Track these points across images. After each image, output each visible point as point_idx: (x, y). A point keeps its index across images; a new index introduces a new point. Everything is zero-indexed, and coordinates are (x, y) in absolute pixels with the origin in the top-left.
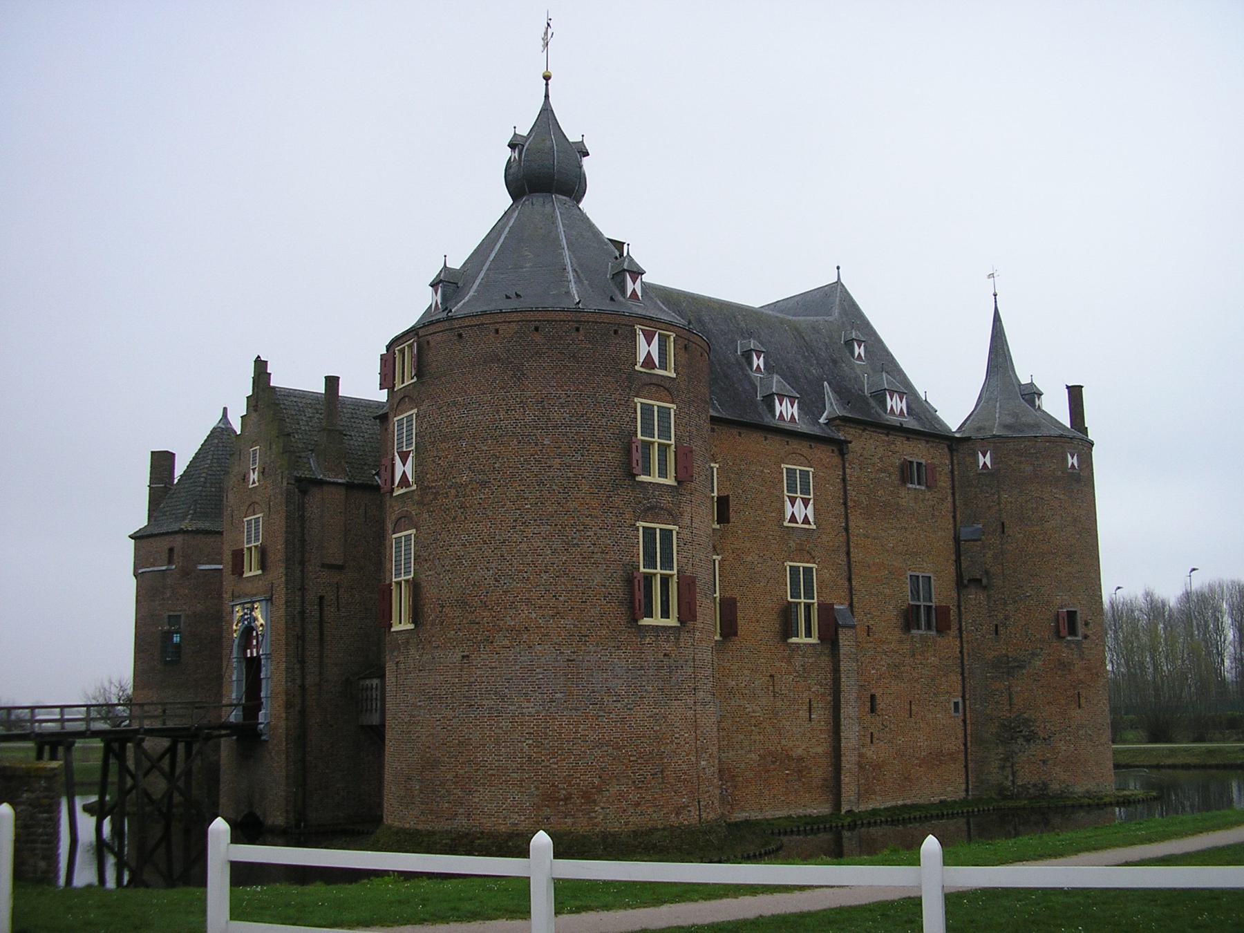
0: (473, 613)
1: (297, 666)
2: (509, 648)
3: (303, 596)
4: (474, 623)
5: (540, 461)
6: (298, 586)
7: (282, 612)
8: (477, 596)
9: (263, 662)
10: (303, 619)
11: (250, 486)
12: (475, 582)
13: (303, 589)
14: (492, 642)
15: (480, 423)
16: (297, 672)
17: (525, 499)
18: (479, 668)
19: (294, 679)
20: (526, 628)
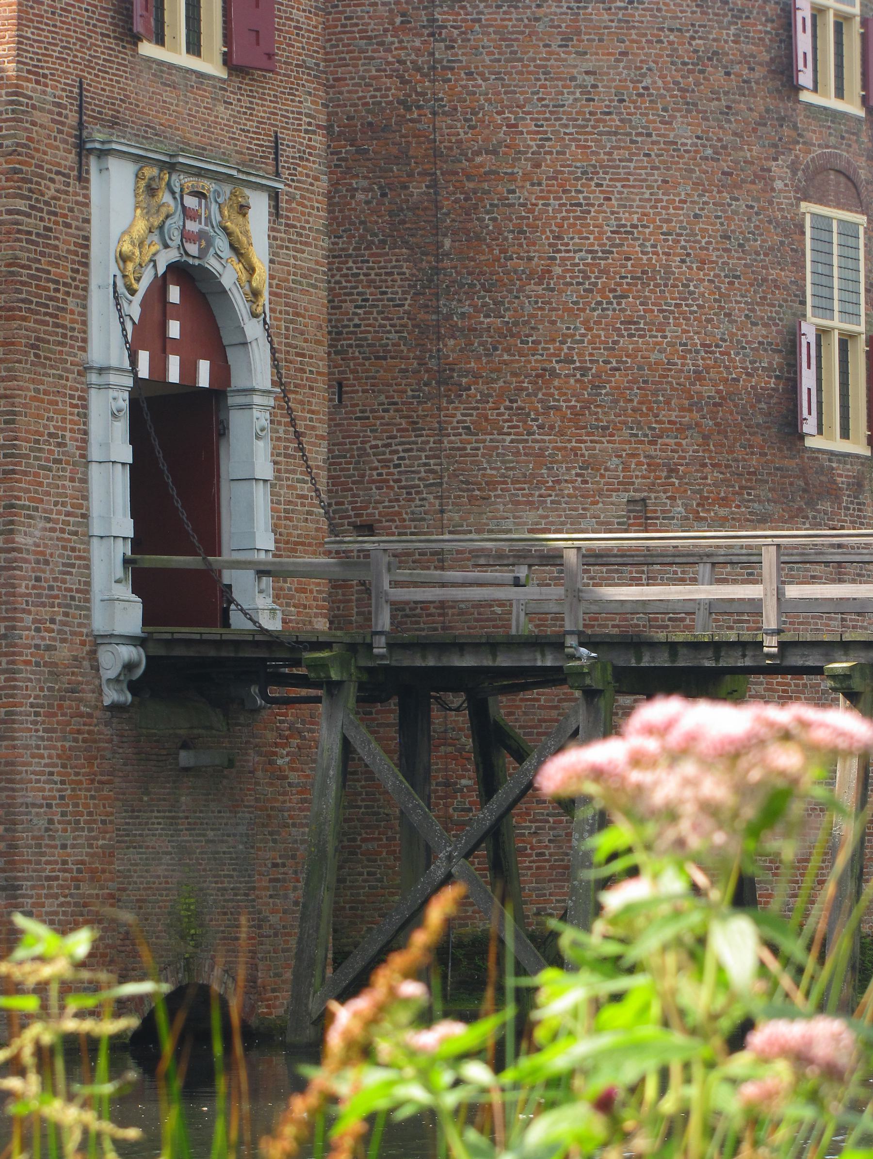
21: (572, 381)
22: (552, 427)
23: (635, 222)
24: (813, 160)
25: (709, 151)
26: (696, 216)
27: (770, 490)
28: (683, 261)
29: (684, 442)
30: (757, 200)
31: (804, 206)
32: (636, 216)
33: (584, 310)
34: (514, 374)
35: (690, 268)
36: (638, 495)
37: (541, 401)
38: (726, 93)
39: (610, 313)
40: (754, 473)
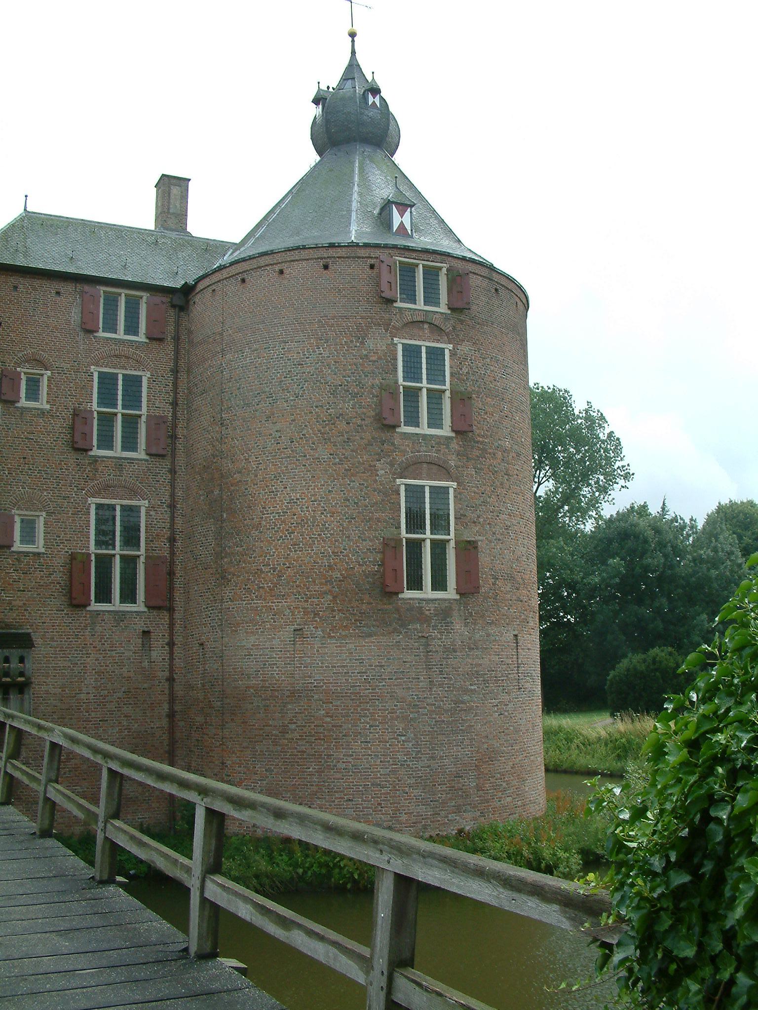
21: (269, 574)
22: (261, 597)
23: (298, 497)
24: (407, 459)
25: (337, 460)
26: (329, 491)
27: (374, 620)
28: (322, 513)
29: (322, 600)
30: (367, 481)
31: (398, 481)
32: (298, 494)
33: (274, 541)
34: (247, 573)
35: (326, 516)
36: (298, 627)
37: (257, 585)
39: (286, 541)
40: (364, 613)
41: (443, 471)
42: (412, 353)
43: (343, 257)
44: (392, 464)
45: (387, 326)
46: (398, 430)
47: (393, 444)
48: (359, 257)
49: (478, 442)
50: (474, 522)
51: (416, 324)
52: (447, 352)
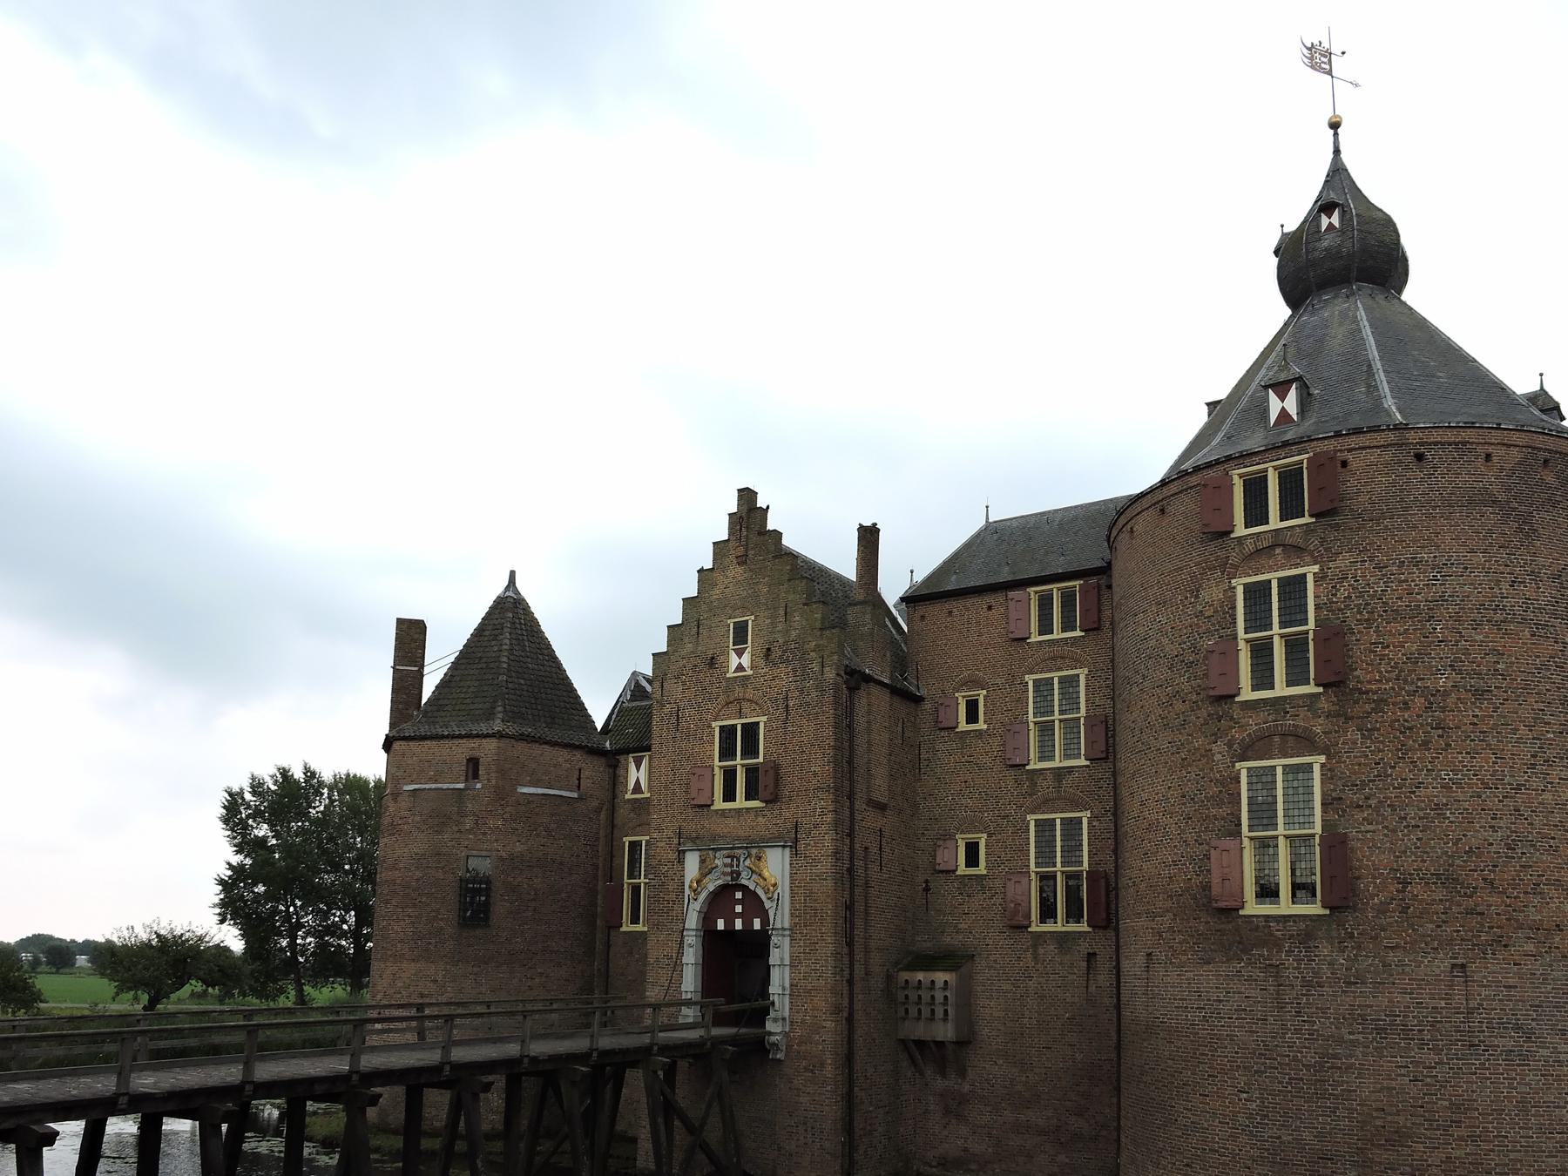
0: (1471, 897)
1: (846, 950)
2: (1535, 956)
3: (852, 848)
4: (1470, 912)
5: (1563, 667)
6: (847, 830)
7: (825, 866)
8: (1476, 871)
9: (774, 940)
10: (852, 879)
11: (728, 675)
12: (1471, 848)
13: (851, 835)
14: (1505, 946)
15: (1468, 597)
16: (846, 960)
17: (1546, 723)
18: (1485, 986)
19: (842, 970)
20: (1558, 926)
35: (1166, 818)
38: (1183, 713)
41: (1306, 742)
42: (1257, 594)
43: (1176, 494)
44: (1230, 745)
45: (1223, 566)
46: (1237, 699)
47: (1232, 718)
48: (1191, 488)
49: (1367, 693)
50: (1359, 806)
51: (1263, 552)
52: (1310, 579)
